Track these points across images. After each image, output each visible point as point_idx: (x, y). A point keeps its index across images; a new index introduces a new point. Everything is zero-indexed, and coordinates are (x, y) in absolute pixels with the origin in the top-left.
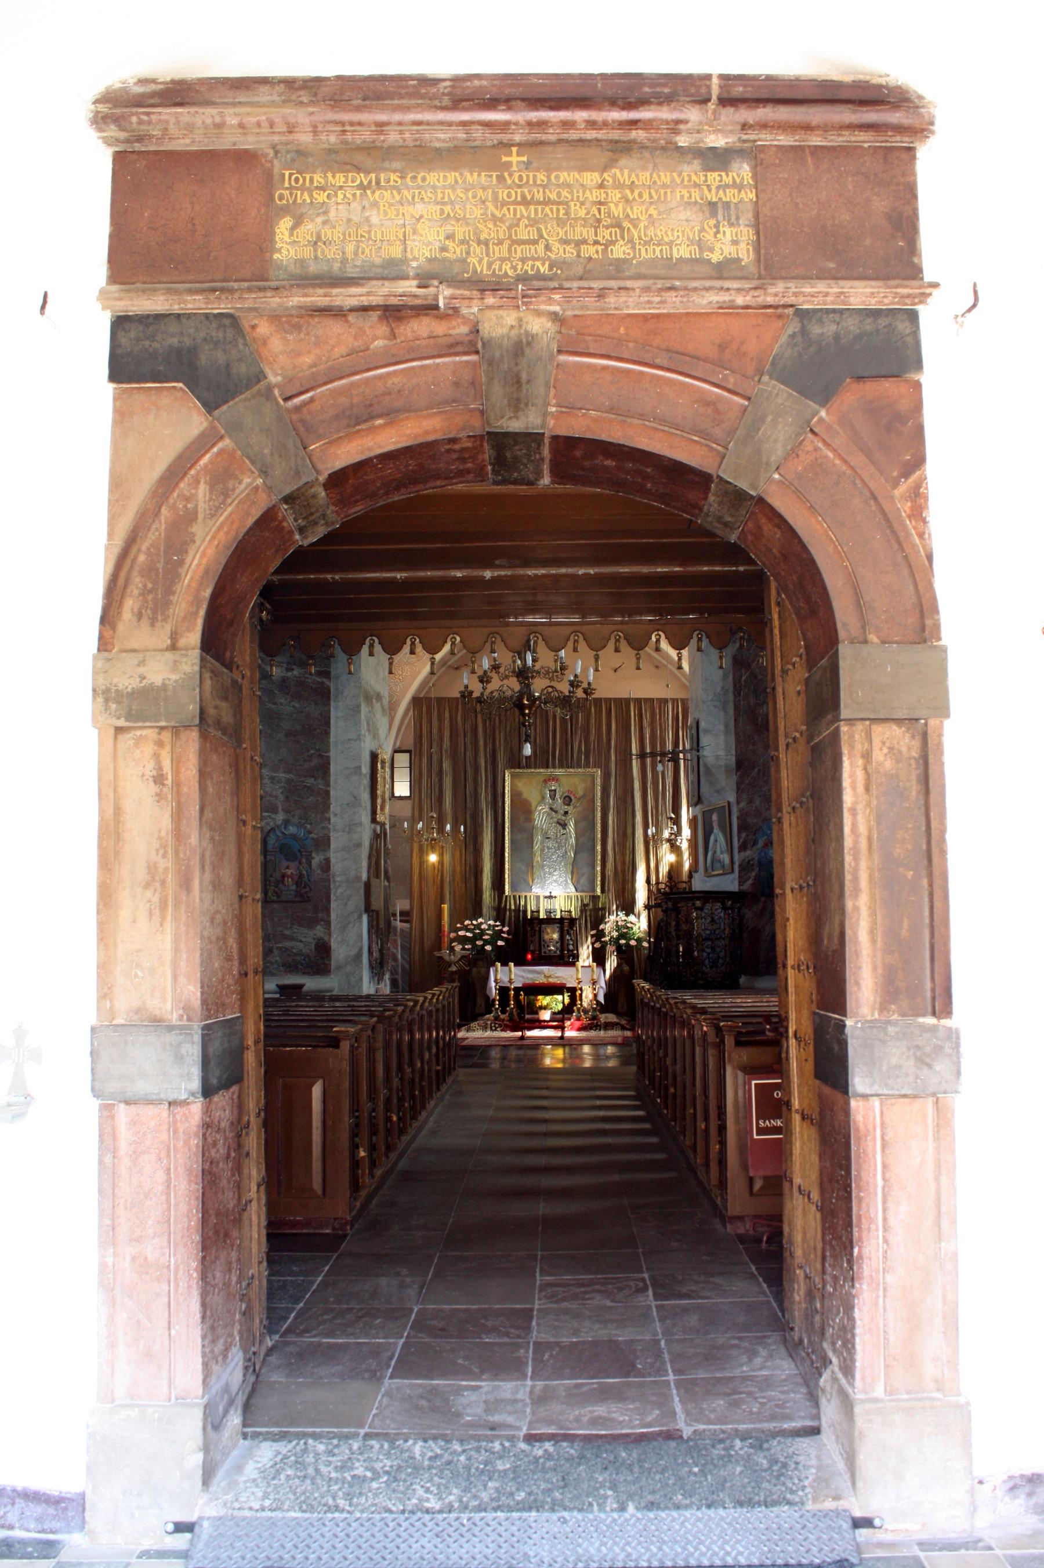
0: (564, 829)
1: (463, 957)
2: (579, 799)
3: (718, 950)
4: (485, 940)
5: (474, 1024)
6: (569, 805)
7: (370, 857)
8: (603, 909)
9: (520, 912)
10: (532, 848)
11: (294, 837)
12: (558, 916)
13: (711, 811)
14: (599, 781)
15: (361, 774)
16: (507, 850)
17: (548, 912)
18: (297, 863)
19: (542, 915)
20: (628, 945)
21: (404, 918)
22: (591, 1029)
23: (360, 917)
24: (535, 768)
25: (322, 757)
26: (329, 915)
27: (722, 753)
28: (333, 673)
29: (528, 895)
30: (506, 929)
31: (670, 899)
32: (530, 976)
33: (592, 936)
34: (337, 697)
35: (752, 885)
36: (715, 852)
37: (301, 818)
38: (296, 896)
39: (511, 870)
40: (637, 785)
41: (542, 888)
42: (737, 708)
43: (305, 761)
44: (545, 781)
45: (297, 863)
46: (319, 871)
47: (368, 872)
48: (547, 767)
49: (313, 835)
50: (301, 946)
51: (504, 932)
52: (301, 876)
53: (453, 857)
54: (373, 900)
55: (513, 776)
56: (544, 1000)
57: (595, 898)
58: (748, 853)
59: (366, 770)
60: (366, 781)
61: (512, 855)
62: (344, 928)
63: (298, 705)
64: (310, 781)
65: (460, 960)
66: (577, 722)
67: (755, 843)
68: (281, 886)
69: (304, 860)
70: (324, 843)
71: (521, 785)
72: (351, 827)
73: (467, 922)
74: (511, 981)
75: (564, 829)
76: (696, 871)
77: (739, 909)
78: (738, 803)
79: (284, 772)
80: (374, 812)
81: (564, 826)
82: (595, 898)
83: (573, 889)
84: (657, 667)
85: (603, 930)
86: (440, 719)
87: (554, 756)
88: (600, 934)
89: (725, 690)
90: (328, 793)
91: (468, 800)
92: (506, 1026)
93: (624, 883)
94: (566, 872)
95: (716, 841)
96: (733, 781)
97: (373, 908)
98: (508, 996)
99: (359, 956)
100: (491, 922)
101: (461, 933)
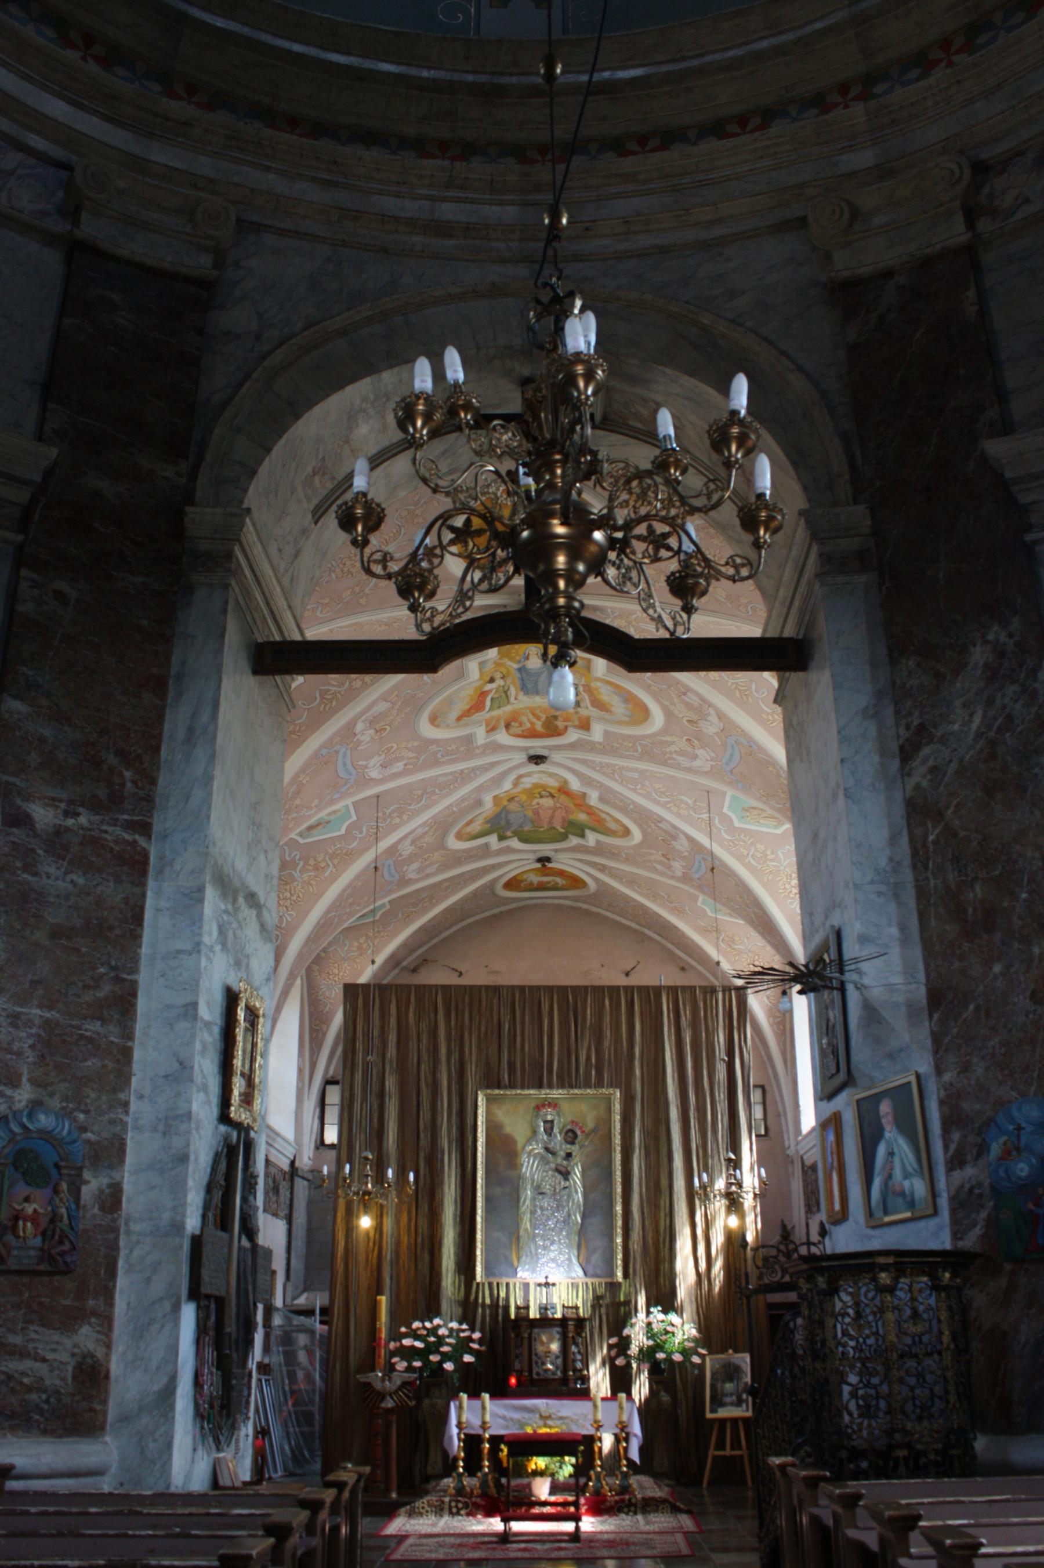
0: (566, 1179)
1: (404, 1384)
2: (587, 1135)
3: (929, 1378)
4: (443, 1354)
5: (421, 1503)
6: (573, 1143)
7: (209, 1189)
8: (627, 1303)
9: (498, 1308)
10: (518, 1207)
11: (46, 1135)
12: (559, 1315)
13: (876, 1099)
14: (617, 1107)
16: (479, 1212)
17: (544, 1309)
18: (48, 1191)
19: (534, 1314)
20: (669, 1360)
21: (325, 1318)
22: (620, 1510)
23: (176, 1308)
24: (522, 1087)
25: (118, 980)
26: (111, 1305)
27: (897, 979)
28: (157, 828)
29: (511, 1281)
30: (477, 1335)
31: (821, 1270)
32: (517, 1416)
33: (610, 1347)
34: (161, 872)
35: (983, 1236)
36: (890, 1177)
37: (66, 1098)
38: (40, 1260)
40: (674, 1113)
41: (534, 1271)
42: (921, 893)
43: (87, 987)
44: (538, 1108)
45: (48, 1191)
46: (96, 1211)
47: (204, 1217)
48: (540, 1086)
49: (89, 1135)
50: (41, 1369)
51: (472, 1340)
52: (54, 1218)
53: (397, 1221)
54: (205, 1273)
55: (489, 1100)
56: (540, 1462)
57: (613, 1287)
58: (969, 1171)
59: (210, 1011)
60: (210, 1038)
61: (487, 1220)
62: (139, 1333)
63: (81, 881)
64: (93, 1027)
65: (400, 1388)
67: (982, 1149)
69: (64, 1186)
71: (501, 1114)
73: (416, 1325)
74: (484, 1426)
75: (566, 1179)
76: (842, 1217)
77: (959, 1289)
78: (939, 1071)
79: (41, 1006)
80: (225, 1102)
81: (566, 1174)
82: (613, 1287)
83: (580, 1272)
84: (683, 969)
85: (629, 1337)
86: (384, 1015)
88: (624, 1344)
89: (895, 864)
90: (127, 1053)
91: (422, 1135)
92: (475, 1504)
93: (658, 1262)
94: (568, 1247)
95: (891, 1154)
96: (924, 1033)
97: (205, 1290)
98: (480, 1451)
99: (169, 1392)
100: (454, 1325)
101: (407, 1342)
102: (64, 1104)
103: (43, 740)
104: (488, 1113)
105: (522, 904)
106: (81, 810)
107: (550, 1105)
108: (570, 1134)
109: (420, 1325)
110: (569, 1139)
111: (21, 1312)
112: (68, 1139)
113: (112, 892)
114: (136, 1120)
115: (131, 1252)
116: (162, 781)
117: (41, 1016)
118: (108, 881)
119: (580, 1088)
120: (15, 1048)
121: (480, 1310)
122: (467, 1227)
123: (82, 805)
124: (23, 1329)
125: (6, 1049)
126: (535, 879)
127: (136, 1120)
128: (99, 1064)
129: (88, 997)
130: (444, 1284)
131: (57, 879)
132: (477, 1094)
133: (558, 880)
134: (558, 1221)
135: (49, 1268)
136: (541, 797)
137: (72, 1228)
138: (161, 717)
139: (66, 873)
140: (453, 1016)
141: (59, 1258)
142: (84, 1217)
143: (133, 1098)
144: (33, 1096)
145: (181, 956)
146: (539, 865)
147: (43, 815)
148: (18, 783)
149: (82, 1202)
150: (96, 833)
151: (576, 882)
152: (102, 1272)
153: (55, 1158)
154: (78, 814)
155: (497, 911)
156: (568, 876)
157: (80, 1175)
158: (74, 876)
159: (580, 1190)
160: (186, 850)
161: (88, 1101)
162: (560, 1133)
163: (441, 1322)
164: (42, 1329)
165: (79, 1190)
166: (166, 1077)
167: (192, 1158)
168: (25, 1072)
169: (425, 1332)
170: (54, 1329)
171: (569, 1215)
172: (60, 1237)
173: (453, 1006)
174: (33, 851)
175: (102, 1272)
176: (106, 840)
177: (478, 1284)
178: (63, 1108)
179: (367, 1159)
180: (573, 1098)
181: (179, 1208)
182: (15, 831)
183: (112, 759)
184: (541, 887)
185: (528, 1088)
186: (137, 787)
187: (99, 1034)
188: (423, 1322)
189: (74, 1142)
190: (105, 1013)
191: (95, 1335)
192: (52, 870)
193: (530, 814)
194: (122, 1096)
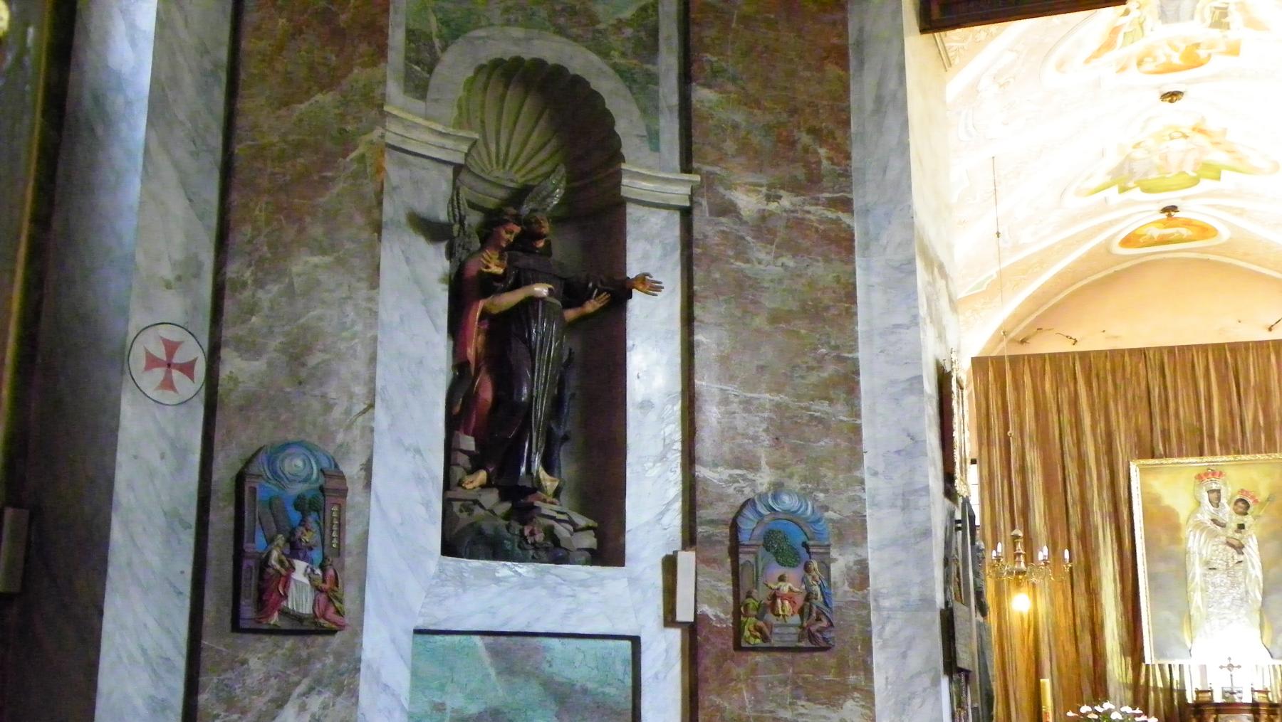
11: (792, 516)
12: (1247, 699)
15: (921, 391)
19: (1218, 699)
23: (936, 683)
24: (1180, 455)
25: (840, 359)
28: (857, 205)
34: (866, 247)
37: (805, 479)
39: (1154, 623)
43: (810, 369)
46: (846, 588)
48: (1201, 454)
49: (830, 514)
52: (808, 597)
53: (1052, 602)
55: (1143, 470)
60: (931, 410)
63: (791, 263)
64: (821, 408)
66: (1247, 380)
68: (770, 617)
70: (854, 529)
72: (908, 498)
79: (770, 391)
80: (949, 478)
81: (1239, 548)
86: (1018, 387)
87: (1211, 437)
90: (857, 430)
100: (1128, 709)
102: (804, 485)
103: (736, 127)
104: (1143, 485)
105: (1144, 260)
106: (782, 192)
107: (1214, 474)
108: (1240, 504)
109: (1089, 709)
110: (1240, 510)
111: (788, 688)
112: (812, 518)
113: (822, 271)
114: (873, 497)
115: (883, 627)
116: (855, 154)
117: (770, 400)
118: (818, 261)
119: (1248, 453)
120: (751, 433)
121: (1152, 694)
122: (1130, 607)
123: (782, 188)
124: (791, 704)
125: (743, 435)
126: (1156, 232)
127: (873, 497)
128: (833, 443)
129: (813, 378)
130: (1109, 666)
131: (768, 264)
132: (1129, 465)
133: (1185, 232)
134: (1234, 599)
135: (810, 645)
136: (1172, 139)
137: (826, 605)
138: (846, 89)
139: (776, 257)
140: (1095, 384)
141: (819, 635)
142: (836, 594)
143: (867, 476)
144: (773, 479)
145: (898, 330)
146: (1164, 216)
147: (748, 202)
148: (719, 172)
149: (832, 580)
150: (799, 215)
151: (1205, 231)
152: (859, 647)
153: (803, 538)
154: (780, 197)
155: (1111, 271)
156: (1197, 226)
157: (829, 553)
158: (784, 260)
159: (1258, 564)
160: (890, 223)
161: (826, 480)
162: (1229, 504)
163: (1113, 707)
164: (809, 703)
165: (828, 569)
166: (898, 452)
167: (933, 533)
168: (763, 455)
169: (1096, 717)
170: (819, 704)
171: (1247, 592)
172: (817, 614)
173: (1094, 373)
174: (742, 238)
175: (859, 647)
176: (809, 220)
177: (1147, 666)
178: (804, 489)
179: (1017, 537)
180: (1243, 464)
181: (926, 582)
182: (723, 219)
183: (805, 139)
184: (1163, 241)
185: (1187, 456)
186: (833, 163)
187: (827, 413)
188: (1092, 706)
189: (819, 521)
190: (831, 392)
191: (860, 709)
192: (762, 256)
193: (1156, 160)
194: (857, 474)
